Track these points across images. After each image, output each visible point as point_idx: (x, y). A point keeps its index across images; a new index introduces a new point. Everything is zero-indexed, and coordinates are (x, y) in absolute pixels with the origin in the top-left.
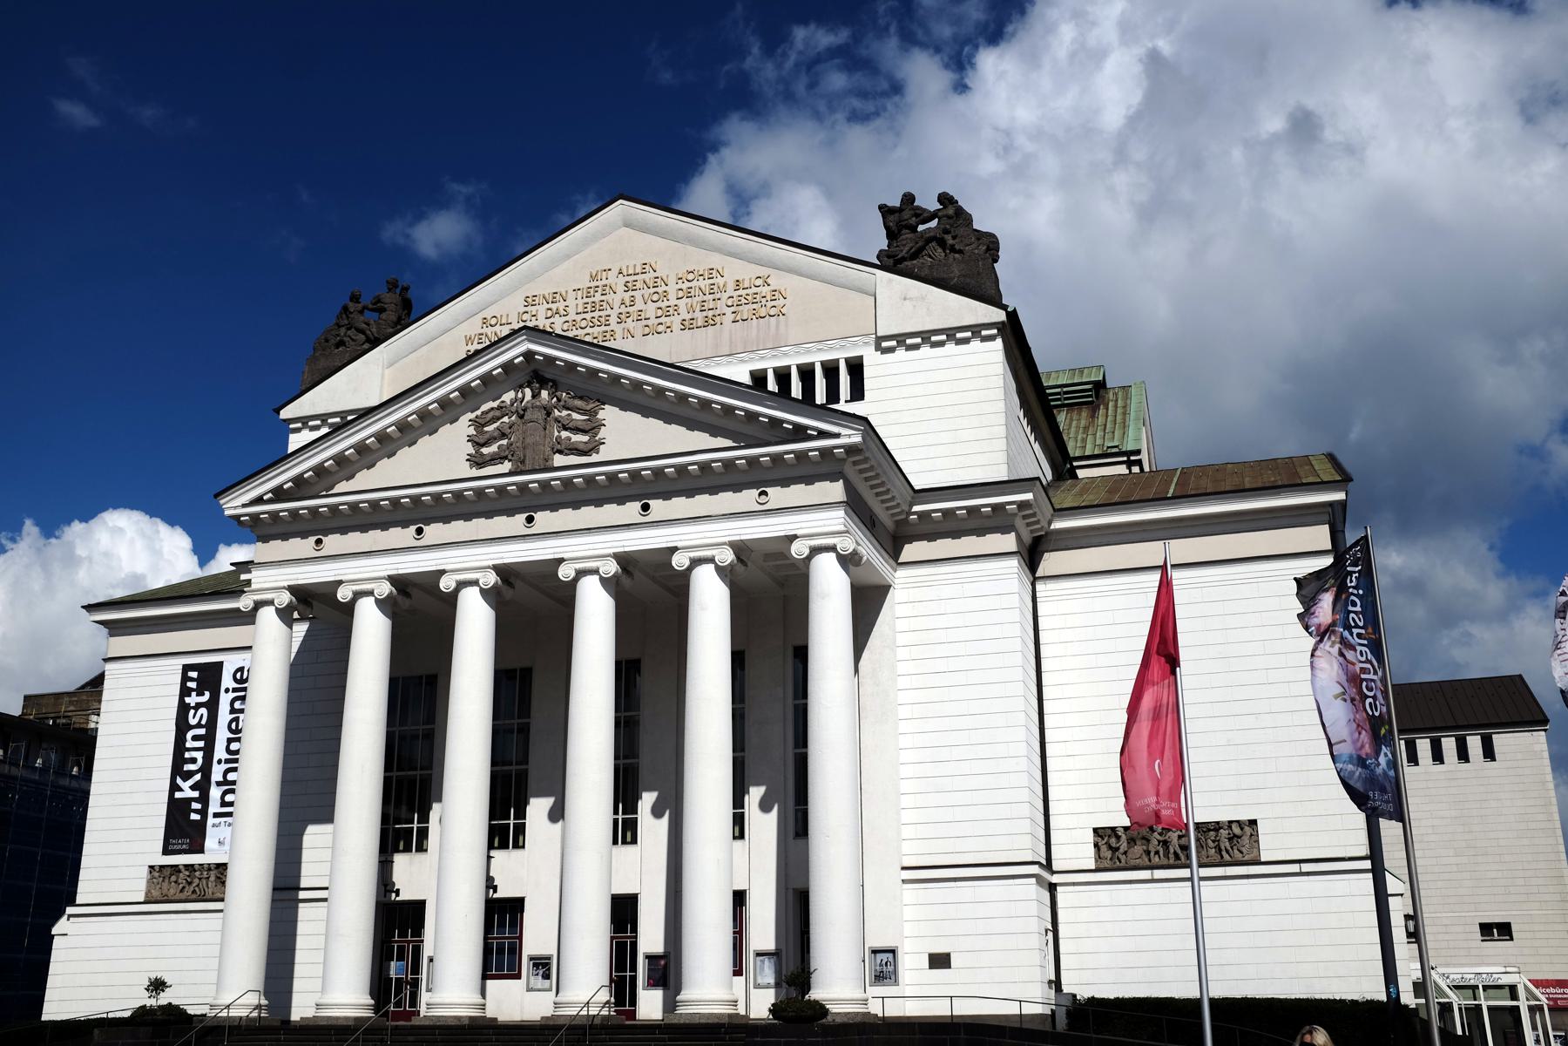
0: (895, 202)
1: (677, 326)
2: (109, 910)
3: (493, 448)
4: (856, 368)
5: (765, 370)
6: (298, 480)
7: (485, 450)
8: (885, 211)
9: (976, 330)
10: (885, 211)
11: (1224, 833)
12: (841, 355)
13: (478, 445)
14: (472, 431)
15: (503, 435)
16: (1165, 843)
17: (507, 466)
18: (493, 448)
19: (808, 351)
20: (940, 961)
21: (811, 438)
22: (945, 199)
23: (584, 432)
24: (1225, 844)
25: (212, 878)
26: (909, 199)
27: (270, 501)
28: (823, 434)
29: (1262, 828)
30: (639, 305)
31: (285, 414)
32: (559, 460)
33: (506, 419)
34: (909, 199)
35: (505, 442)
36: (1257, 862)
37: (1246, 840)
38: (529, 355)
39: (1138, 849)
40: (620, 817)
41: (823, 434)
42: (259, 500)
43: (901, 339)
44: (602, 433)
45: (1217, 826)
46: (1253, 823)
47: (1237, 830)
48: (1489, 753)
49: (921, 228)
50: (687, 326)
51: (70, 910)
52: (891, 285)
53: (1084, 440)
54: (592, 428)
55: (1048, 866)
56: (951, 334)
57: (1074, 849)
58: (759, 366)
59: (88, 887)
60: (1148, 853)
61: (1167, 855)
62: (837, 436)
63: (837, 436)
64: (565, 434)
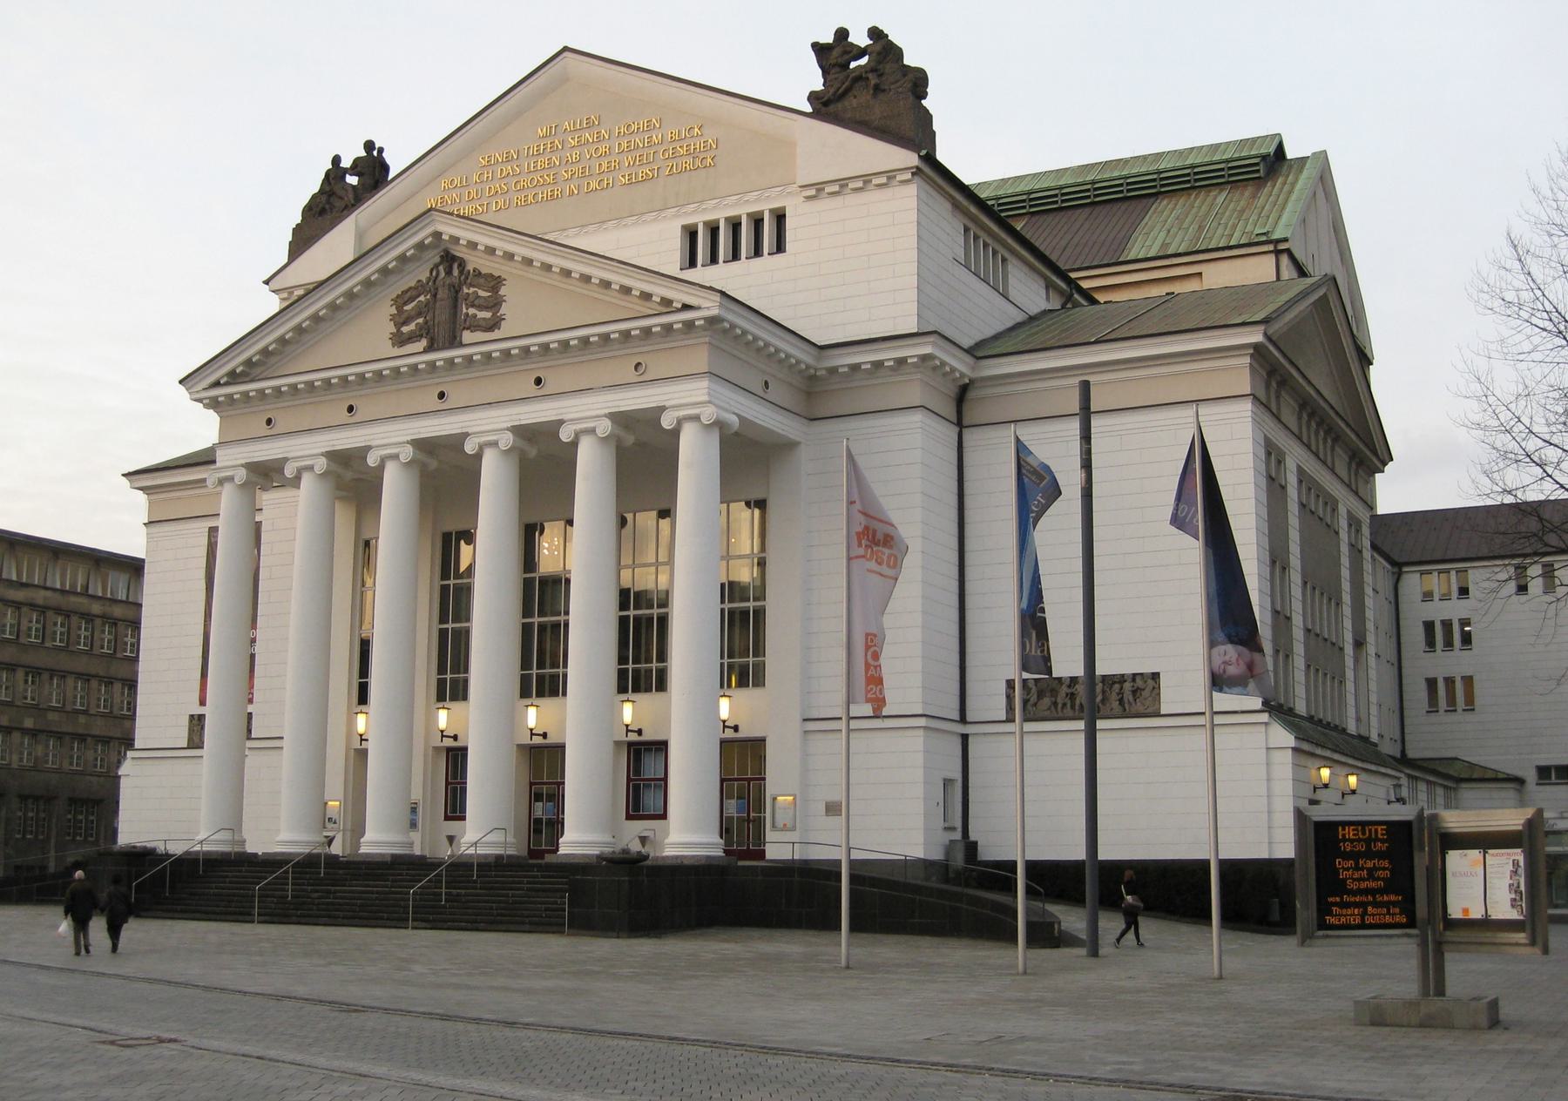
0: (828, 38)
2: (161, 753)
3: (412, 326)
4: (780, 218)
5: (717, 221)
6: (248, 363)
7: (405, 329)
8: (819, 49)
9: (890, 175)
10: (819, 49)
11: (1128, 686)
12: (765, 207)
13: (399, 325)
14: (394, 310)
15: (419, 315)
16: (1072, 696)
17: (424, 343)
18: (412, 326)
19: (736, 204)
21: (678, 310)
22: (876, 33)
23: (487, 308)
24: (1128, 696)
26: (842, 34)
27: (227, 384)
28: (686, 307)
29: (1164, 681)
31: (275, 284)
32: (467, 336)
33: (422, 298)
34: (842, 34)
35: (421, 320)
36: (1158, 715)
37: (1146, 693)
39: (1047, 701)
40: (726, 661)
41: (686, 307)
42: (217, 384)
43: (819, 187)
45: (1122, 679)
46: (1155, 676)
47: (1139, 682)
48: (1549, 587)
49: (853, 65)
51: (130, 754)
53: (1235, 227)
54: (495, 303)
55: (963, 719)
56: (867, 180)
57: (989, 700)
58: (690, 221)
59: (144, 734)
60: (1055, 704)
61: (1073, 707)
62: (699, 308)
63: (699, 308)
64: (472, 311)
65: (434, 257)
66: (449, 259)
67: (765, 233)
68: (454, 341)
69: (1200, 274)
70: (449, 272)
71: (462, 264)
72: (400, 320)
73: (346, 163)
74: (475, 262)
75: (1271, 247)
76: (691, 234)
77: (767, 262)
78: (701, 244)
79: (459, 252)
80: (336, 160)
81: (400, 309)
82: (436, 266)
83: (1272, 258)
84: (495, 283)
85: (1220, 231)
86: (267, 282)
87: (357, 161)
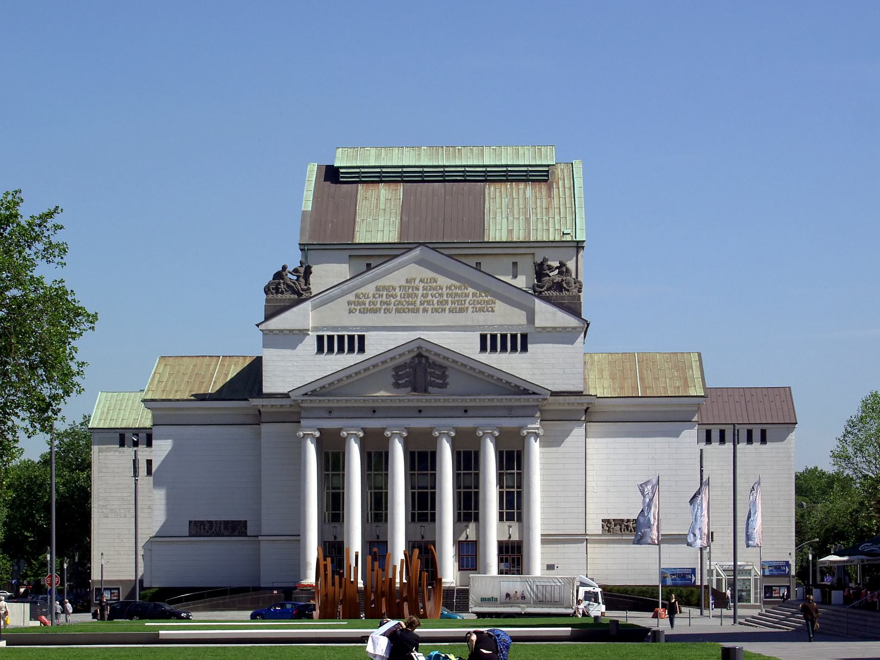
1: (447, 311)
3: (403, 381)
7: (400, 382)
13: (396, 380)
14: (393, 373)
16: (627, 527)
17: (409, 389)
18: (403, 381)
20: (550, 567)
21: (530, 394)
25: (222, 527)
28: (534, 393)
30: (430, 298)
31: (262, 327)
32: (430, 389)
38: (419, 348)
39: (618, 527)
41: (534, 393)
42: (306, 394)
44: (448, 381)
50: (451, 311)
52: (540, 306)
54: (444, 376)
64: (432, 379)
65: (413, 354)
66: (420, 355)
67: (518, 343)
68: (426, 391)
69: (533, 254)
70: (420, 362)
71: (427, 358)
72: (397, 377)
73: (290, 268)
74: (432, 358)
75: (575, 244)
76: (483, 338)
77: (517, 355)
78: (489, 343)
79: (425, 354)
80: (284, 268)
81: (397, 373)
82: (413, 358)
83: (575, 249)
84: (443, 368)
85: (540, 226)
86: (258, 325)
87: (296, 270)
